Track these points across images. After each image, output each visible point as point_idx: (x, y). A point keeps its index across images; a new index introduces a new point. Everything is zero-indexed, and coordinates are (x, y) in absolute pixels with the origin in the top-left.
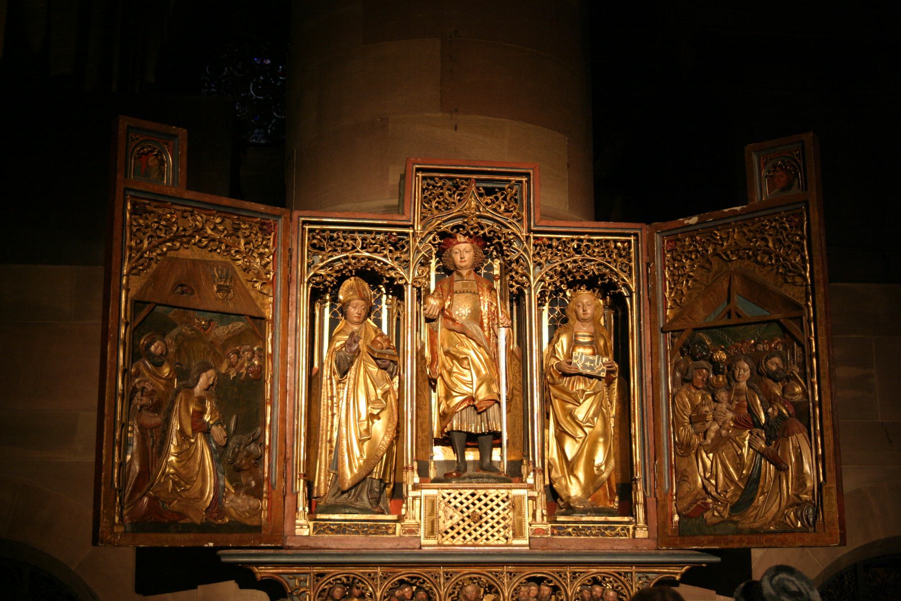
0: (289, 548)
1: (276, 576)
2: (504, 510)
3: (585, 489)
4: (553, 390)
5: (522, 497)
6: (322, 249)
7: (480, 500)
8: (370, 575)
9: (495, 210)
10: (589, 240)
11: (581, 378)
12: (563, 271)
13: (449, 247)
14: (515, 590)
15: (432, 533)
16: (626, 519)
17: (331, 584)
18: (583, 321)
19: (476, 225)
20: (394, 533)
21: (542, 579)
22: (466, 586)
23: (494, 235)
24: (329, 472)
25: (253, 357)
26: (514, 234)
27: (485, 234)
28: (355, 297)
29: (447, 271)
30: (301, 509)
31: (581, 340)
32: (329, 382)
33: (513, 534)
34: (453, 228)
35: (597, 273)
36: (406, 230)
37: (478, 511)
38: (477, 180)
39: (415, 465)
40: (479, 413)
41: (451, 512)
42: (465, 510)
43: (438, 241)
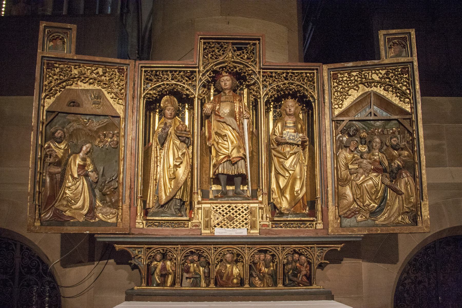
0: (133, 234)
1: (126, 249)
2: (246, 214)
3: (289, 203)
4: (273, 152)
5: (256, 208)
6: (151, 80)
7: (233, 209)
8: (174, 248)
9: (242, 58)
10: (292, 73)
11: (288, 145)
12: (279, 89)
13: (219, 79)
14: (252, 256)
15: (207, 226)
16: (311, 219)
17: (155, 253)
18: (289, 115)
20: (188, 227)
21: (267, 250)
22: (226, 255)
23: (242, 71)
24: (155, 196)
25: (113, 137)
27: (237, 71)
28: (169, 105)
29: (218, 91)
30: (139, 214)
31: (288, 125)
32: (155, 149)
33: (251, 227)
34: (220, 68)
35: (296, 90)
36: (195, 70)
37: (232, 215)
38: (233, 44)
39: (199, 191)
41: (217, 216)
42: (225, 215)
43: (212, 75)
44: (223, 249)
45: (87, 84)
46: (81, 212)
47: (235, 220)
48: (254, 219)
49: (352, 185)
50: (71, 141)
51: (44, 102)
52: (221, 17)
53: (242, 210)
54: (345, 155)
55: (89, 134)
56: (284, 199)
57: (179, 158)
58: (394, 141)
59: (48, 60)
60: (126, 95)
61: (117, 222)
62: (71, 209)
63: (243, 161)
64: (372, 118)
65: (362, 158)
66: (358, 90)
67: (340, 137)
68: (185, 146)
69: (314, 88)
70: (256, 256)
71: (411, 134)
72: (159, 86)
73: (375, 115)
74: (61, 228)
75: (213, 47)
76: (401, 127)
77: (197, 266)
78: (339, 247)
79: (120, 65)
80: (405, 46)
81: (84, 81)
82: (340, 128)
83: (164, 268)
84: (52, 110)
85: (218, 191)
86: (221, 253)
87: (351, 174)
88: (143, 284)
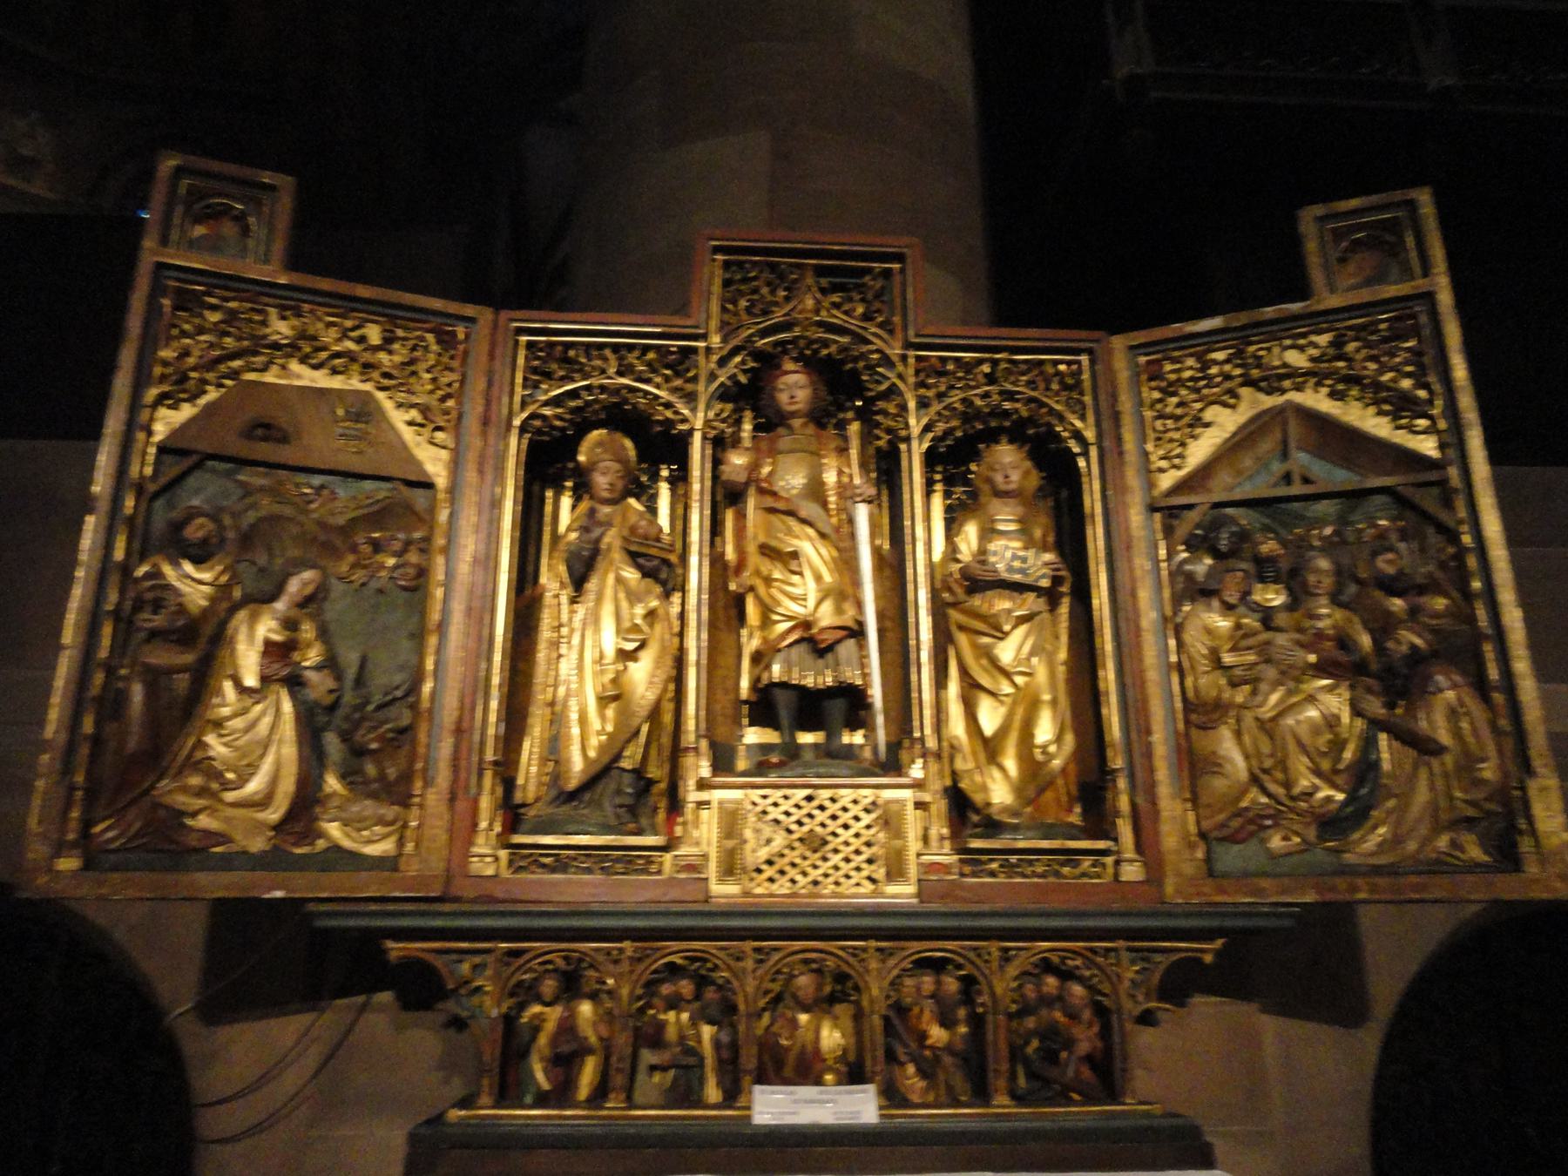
0: (457, 900)
2: (868, 827)
3: (1019, 790)
7: (822, 808)
8: (609, 954)
9: (846, 313)
14: (892, 984)
15: (730, 868)
16: (1101, 845)
17: (535, 971)
20: (659, 872)
21: (945, 961)
28: (606, 456)
30: (483, 825)
31: (1001, 527)
37: (819, 830)
38: (820, 271)
39: (704, 744)
41: (767, 831)
42: (794, 827)
44: (785, 957)
46: (261, 816)
47: (830, 847)
48: (898, 843)
51: (152, 419)
53: (855, 810)
55: (315, 539)
56: (996, 773)
57: (635, 628)
58: (1385, 565)
60: (460, 417)
61: (400, 855)
62: (220, 807)
63: (851, 643)
67: (1185, 561)
68: (658, 589)
70: (909, 982)
71: (1453, 537)
72: (574, 394)
73: (1306, 481)
74: (170, 878)
75: (755, 278)
76: (1408, 514)
77: (691, 1018)
78: (1209, 951)
83: (567, 1028)
85: (765, 748)
86: (778, 972)
88: (485, 1099)
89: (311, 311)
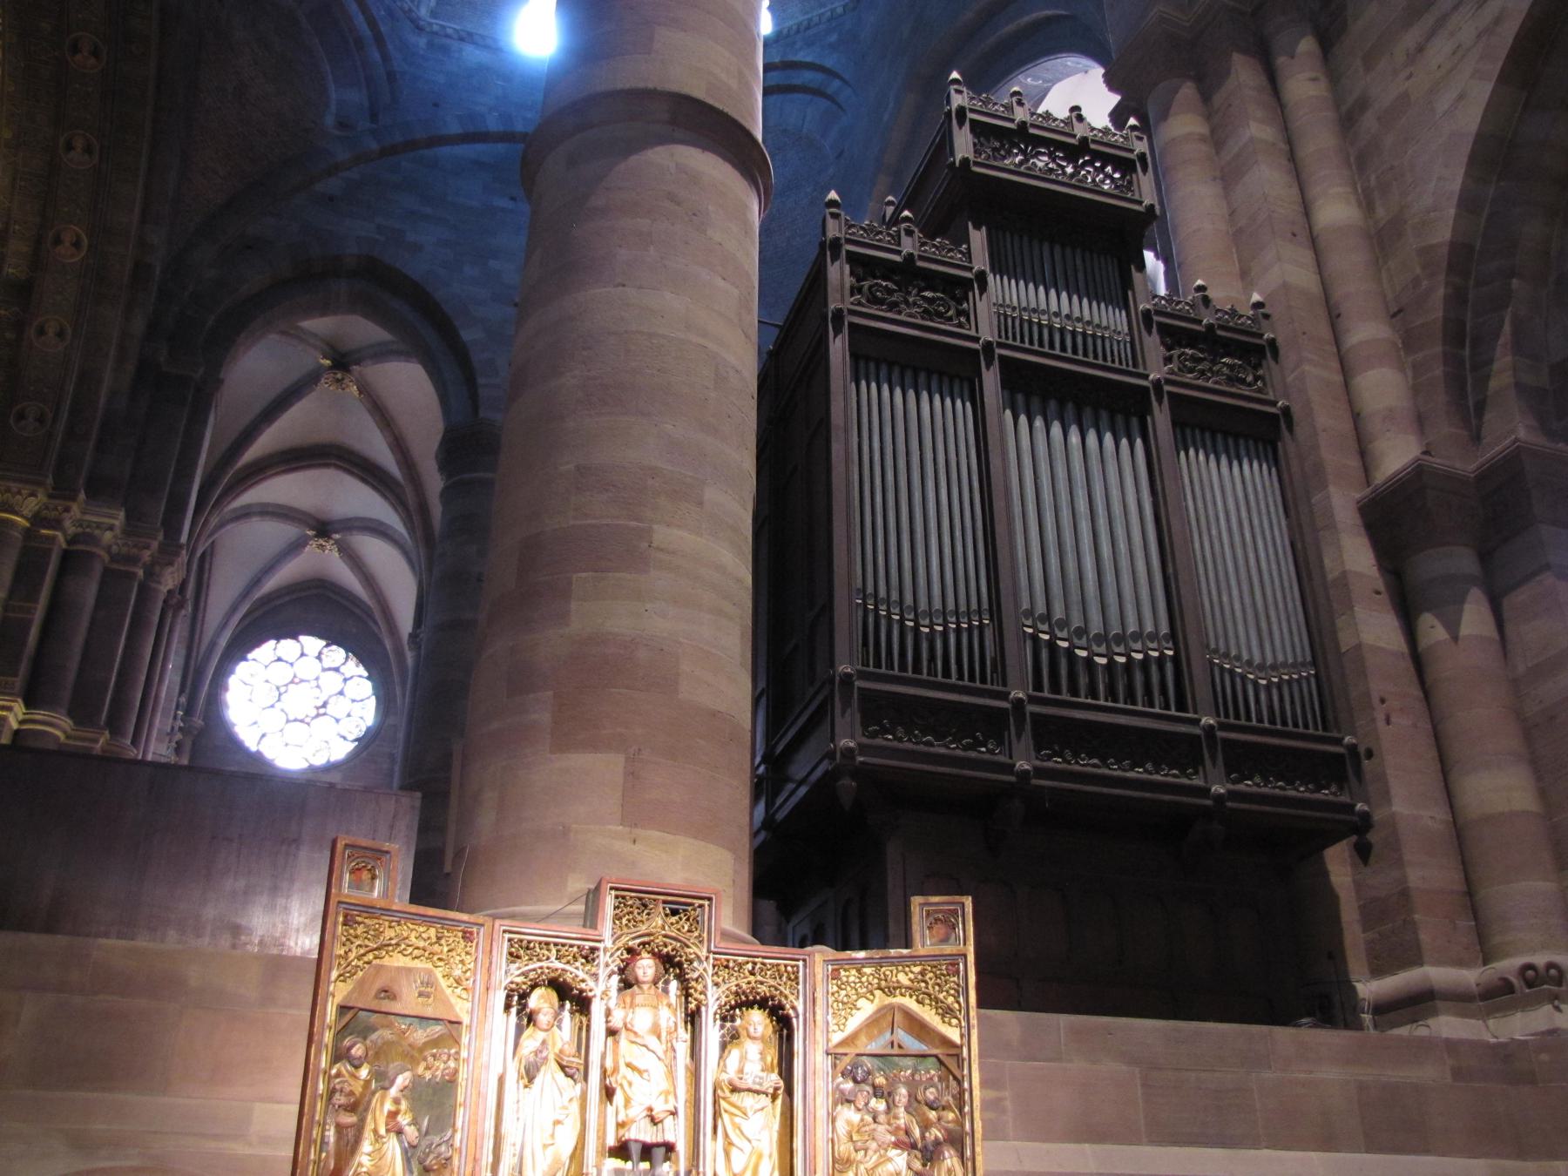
6: (518, 957)
9: (679, 930)
18: (754, 1038)
19: (661, 943)
25: (449, 1059)
26: (695, 953)
29: (627, 984)
35: (768, 994)
38: (665, 902)
40: (655, 1124)
43: (625, 956)
45: (409, 957)
49: (857, 1170)
50: (376, 1064)
52: (621, 827)
54: (848, 1115)
58: (931, 1094)
59: (347, 909)
64: (896, 1051)
65: (875, 1122)
66: (872, 1001)
69: (798, 992)
71: (959, 1082)
75: (631, 907)
76: (943, 1068)
79: (467, 925)
80: (954, 924)
81: (405, 953)
82: (840, 1067)
84: (351, 1004)
87: (856, 1151)
89: (405, 924)
